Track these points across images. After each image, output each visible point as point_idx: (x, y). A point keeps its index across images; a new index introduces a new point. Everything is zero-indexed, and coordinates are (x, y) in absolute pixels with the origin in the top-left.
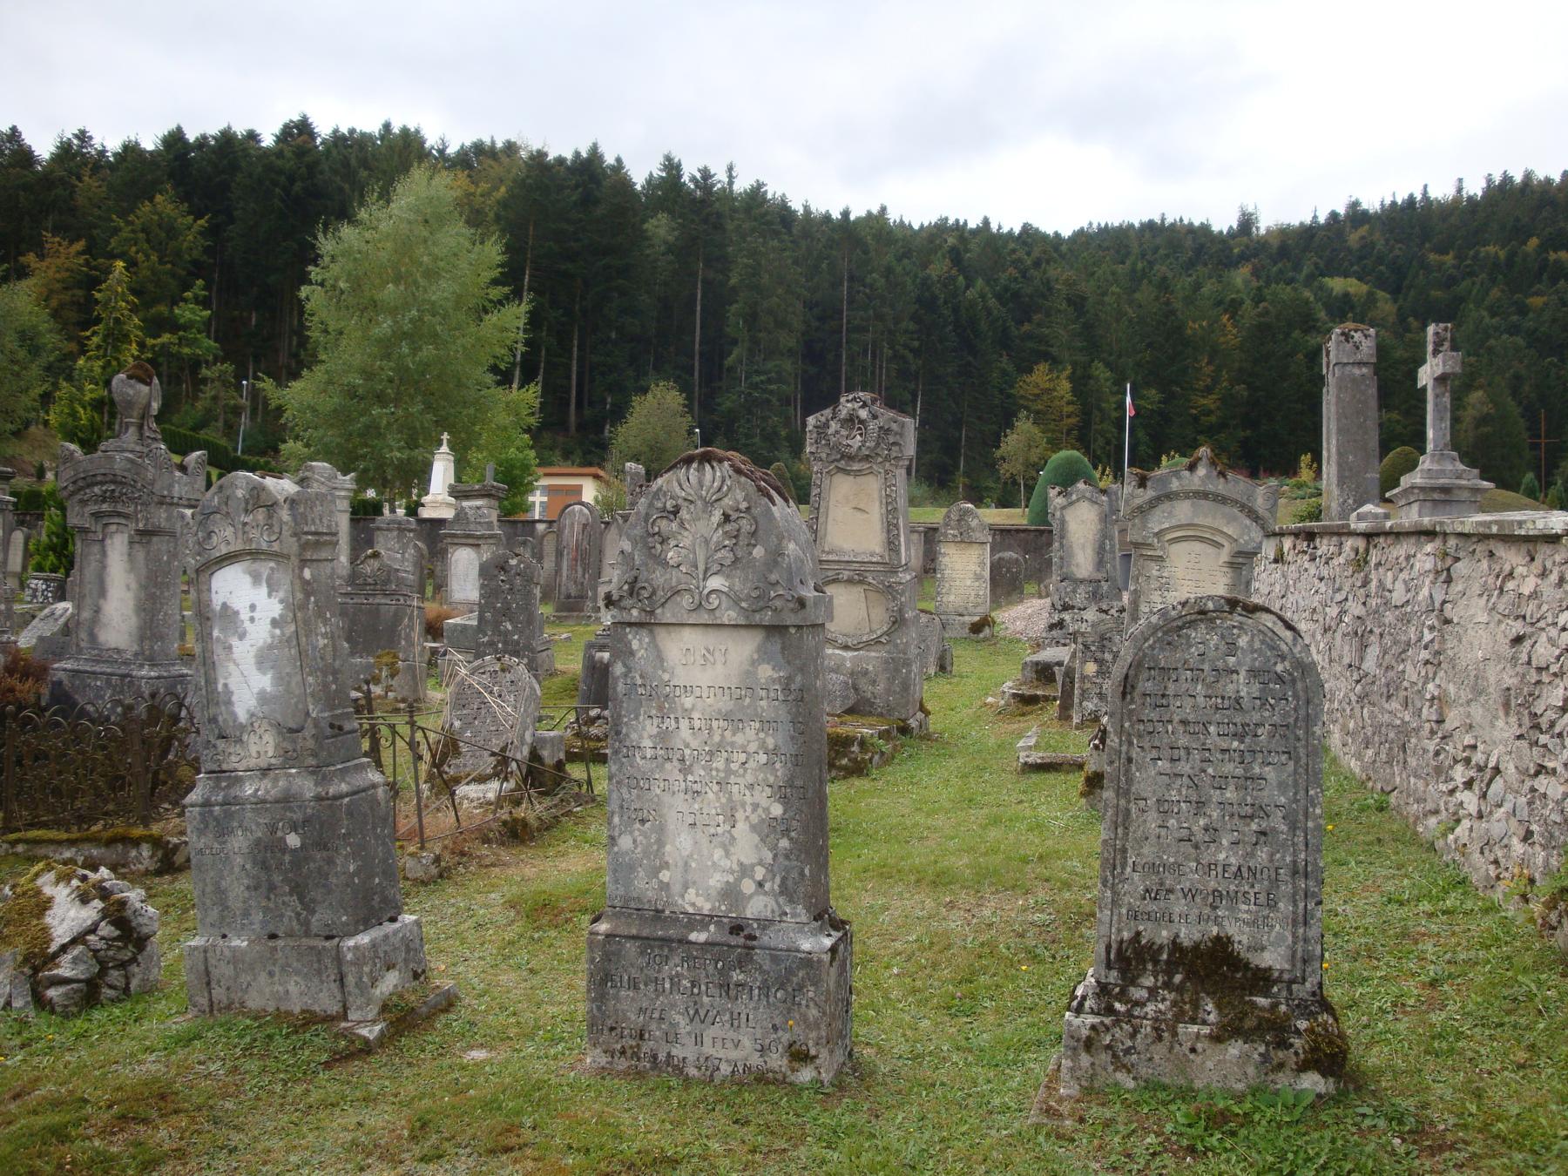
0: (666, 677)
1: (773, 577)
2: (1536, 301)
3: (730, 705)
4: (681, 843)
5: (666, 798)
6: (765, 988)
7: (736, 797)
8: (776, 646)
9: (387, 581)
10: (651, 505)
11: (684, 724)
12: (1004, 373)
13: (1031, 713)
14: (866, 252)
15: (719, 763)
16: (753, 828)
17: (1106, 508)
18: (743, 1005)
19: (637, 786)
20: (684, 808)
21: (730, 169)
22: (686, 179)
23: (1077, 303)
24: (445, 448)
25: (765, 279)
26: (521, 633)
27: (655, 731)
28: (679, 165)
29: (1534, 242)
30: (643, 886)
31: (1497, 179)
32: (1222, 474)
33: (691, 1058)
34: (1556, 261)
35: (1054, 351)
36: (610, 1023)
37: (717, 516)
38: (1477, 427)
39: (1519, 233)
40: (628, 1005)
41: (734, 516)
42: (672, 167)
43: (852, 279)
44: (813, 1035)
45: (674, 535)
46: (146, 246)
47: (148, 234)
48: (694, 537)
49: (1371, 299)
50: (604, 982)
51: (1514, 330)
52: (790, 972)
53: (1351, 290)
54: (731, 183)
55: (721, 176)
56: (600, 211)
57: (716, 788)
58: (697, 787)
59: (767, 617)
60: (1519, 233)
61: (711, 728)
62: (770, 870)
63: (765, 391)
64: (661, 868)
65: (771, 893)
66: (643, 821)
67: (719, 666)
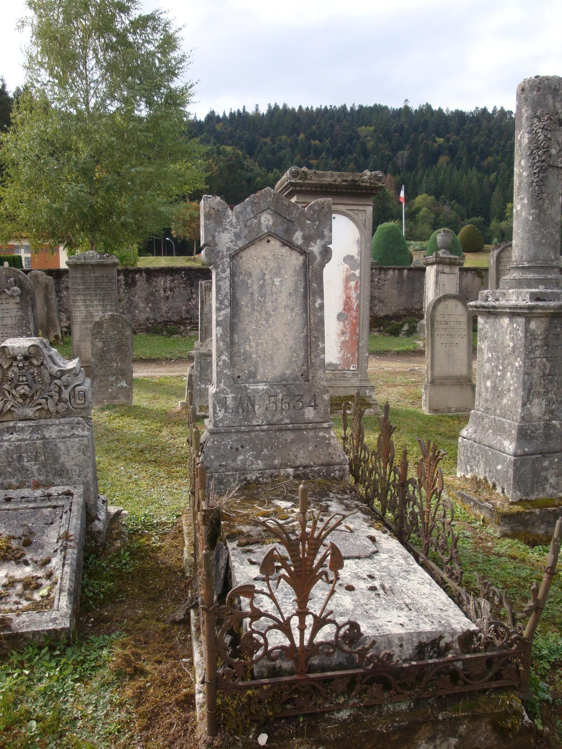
34: (315, 145)
60: (295, 131)
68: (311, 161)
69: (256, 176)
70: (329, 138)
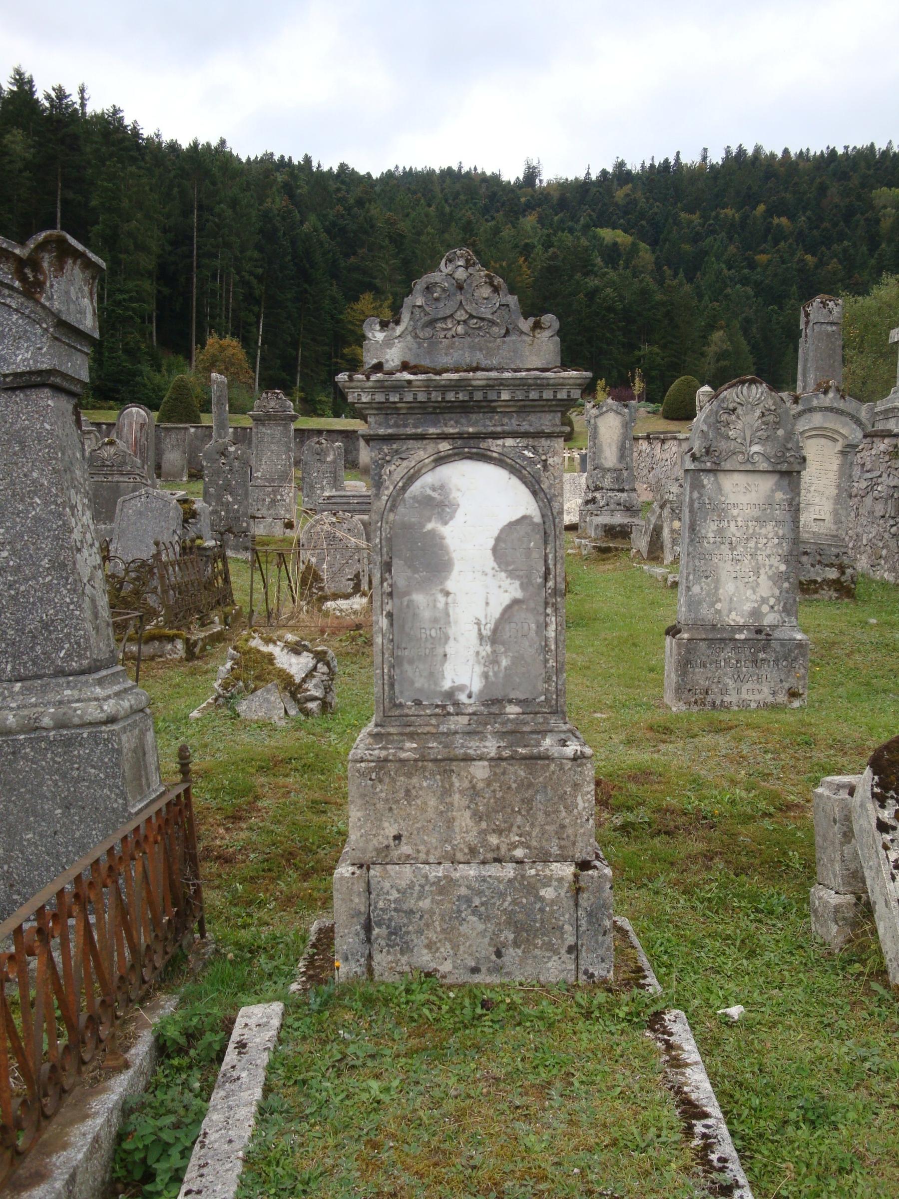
0: (723, 499)
1: (789, 446)
2: (762, 258)
3: (759, 513)
4: (728, 588)
5: (721, 564)
6: (776, 661)
7: (760, 562)
8: (785, 482)
9: (124, 463)
10: (719, 406)
11: (733, 524)
12: (334, 300)
13: (608, 559)
14: (214, 184)
15: (752, 544)
16: (770, 578)
17: (627, 418)
18: (765, 670)
19: (705, 559)
20: (731, 569)
23: (397, 240)
25: (125, 204)
26: (240, 503)
27: (715, 528)
29: (762, 208)
30: (706, 612)
31: (734, 151)
32: (843, 397)
33: (734, 701)
34: (778, 225)
35: (378, 282)
36: (688, 687)
37: (758, 413)
38: (718, 361)
39: (749, 199)
40: (700, 677)
41: (767, 413)
43: (201, 208)
44: (801, 683)
45: (733, 422)
48: (747, 423)
49: (634, 248)
50: (686, 665)
51: (745, 281)
52: (790, 651)
53: (619, 240)
57: (749, 557)
58: (739, 557)
59: (784, 467)
60: (749, 199)
61: (747, 526)
62: (778, 600)
63: (127, 309)
64: (716, 602)
65: (779, 612)
66: (707, 577)
67: (753, 493)
68: (758, 257)
69: (605, 286)
70: (809, 213)
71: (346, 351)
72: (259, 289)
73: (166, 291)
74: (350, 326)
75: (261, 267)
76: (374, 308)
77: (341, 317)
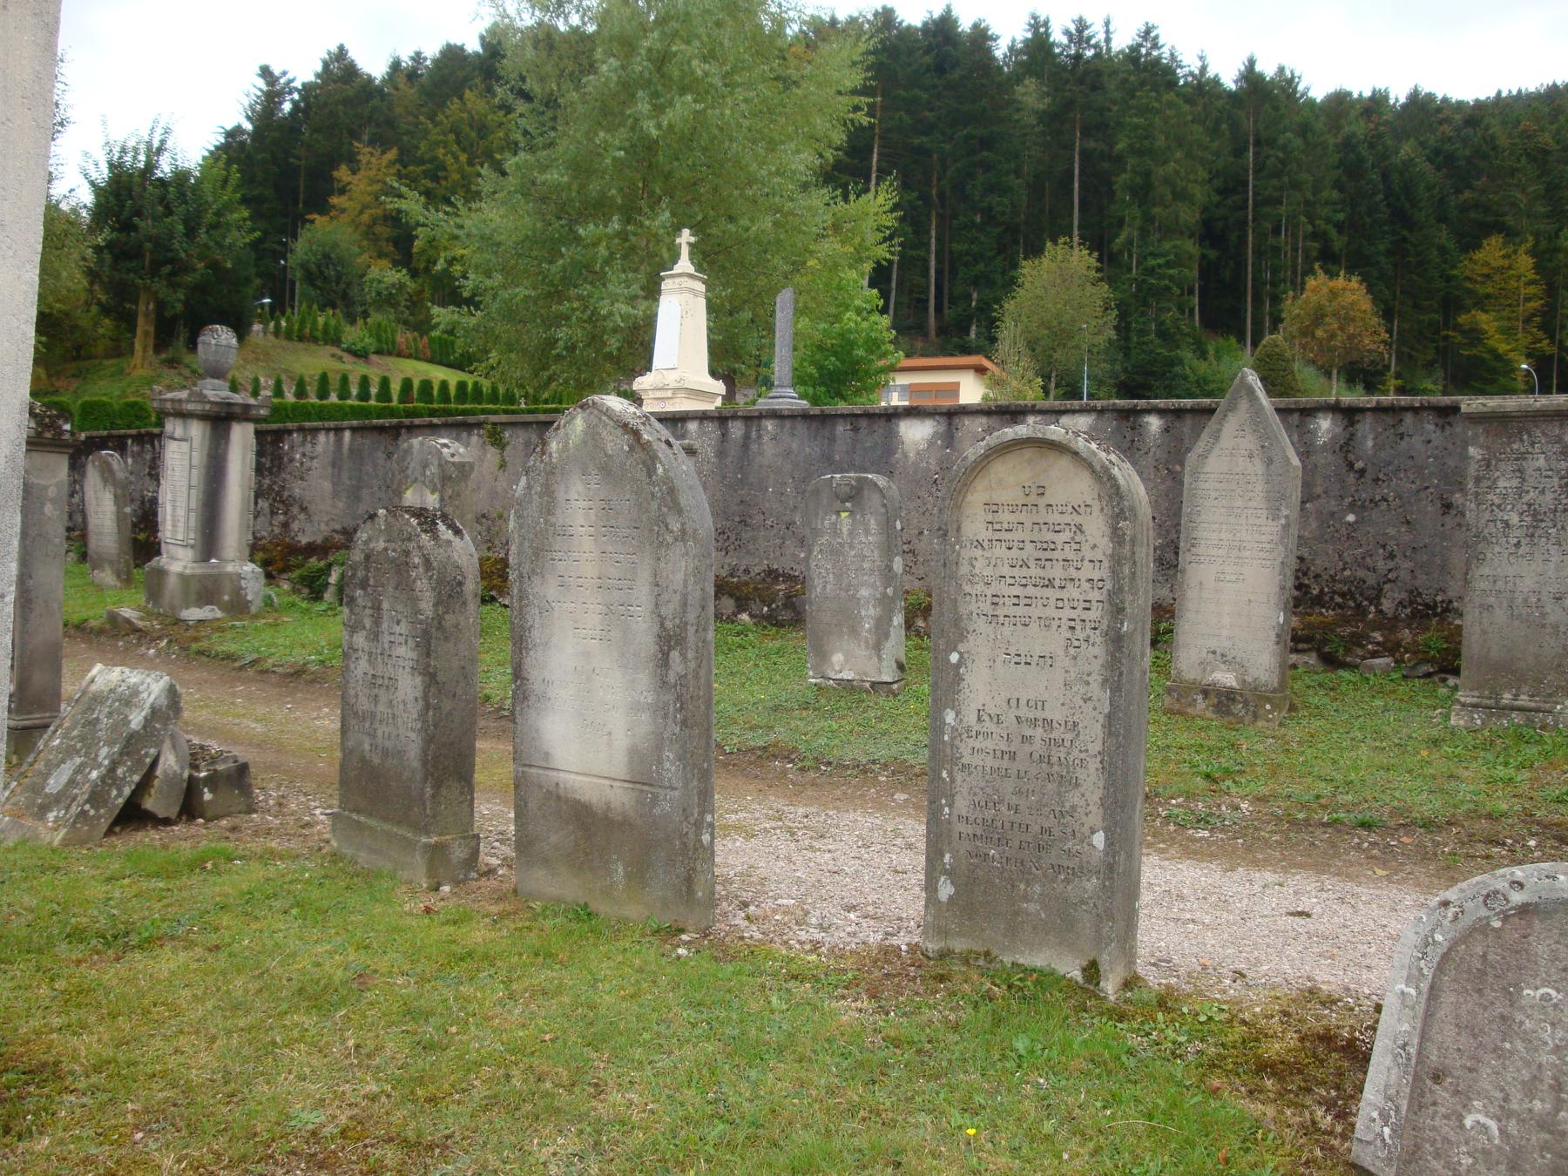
12: (1442, 250)
14: (1276, 108)
21: (1107, 24)
22: (1057, 36)
24: (684, 264)
28: (1046, 24)
35: (1510, 220)
42: (1039, 30)
43: (1258, 143)
46: (455, 148)
47: (457, 135)
54: (1108, 40)
55: (1097, 32)
56: (956, 74)
63: (1161, 277)
71: (1462, 319)
72: (1339, 242)
73: (1213, 254)
74: (1468, 285)
75: (1342, 210)
76: (1504, 257)
77: (1455, 272)
